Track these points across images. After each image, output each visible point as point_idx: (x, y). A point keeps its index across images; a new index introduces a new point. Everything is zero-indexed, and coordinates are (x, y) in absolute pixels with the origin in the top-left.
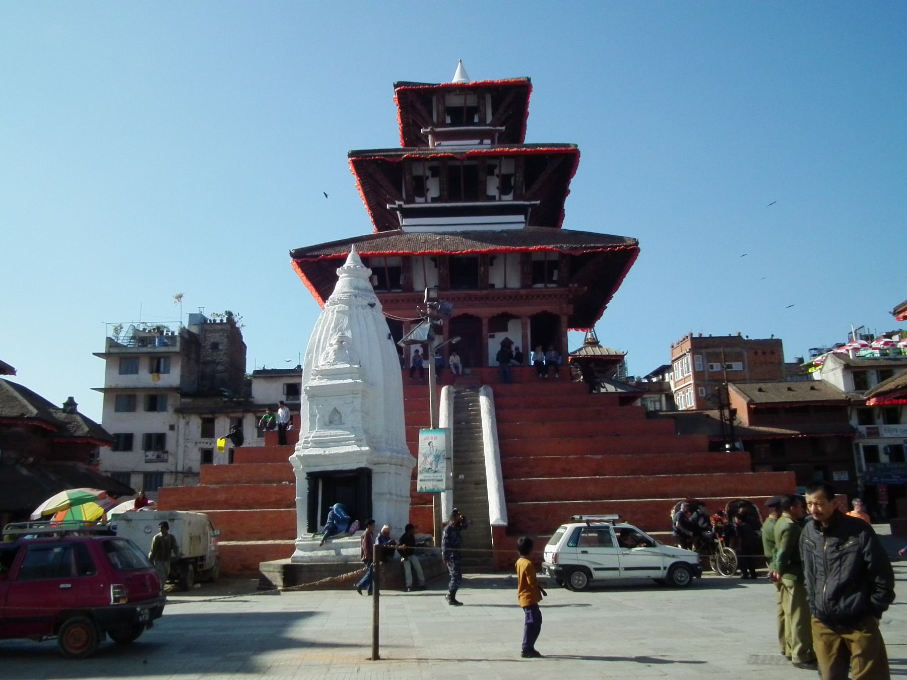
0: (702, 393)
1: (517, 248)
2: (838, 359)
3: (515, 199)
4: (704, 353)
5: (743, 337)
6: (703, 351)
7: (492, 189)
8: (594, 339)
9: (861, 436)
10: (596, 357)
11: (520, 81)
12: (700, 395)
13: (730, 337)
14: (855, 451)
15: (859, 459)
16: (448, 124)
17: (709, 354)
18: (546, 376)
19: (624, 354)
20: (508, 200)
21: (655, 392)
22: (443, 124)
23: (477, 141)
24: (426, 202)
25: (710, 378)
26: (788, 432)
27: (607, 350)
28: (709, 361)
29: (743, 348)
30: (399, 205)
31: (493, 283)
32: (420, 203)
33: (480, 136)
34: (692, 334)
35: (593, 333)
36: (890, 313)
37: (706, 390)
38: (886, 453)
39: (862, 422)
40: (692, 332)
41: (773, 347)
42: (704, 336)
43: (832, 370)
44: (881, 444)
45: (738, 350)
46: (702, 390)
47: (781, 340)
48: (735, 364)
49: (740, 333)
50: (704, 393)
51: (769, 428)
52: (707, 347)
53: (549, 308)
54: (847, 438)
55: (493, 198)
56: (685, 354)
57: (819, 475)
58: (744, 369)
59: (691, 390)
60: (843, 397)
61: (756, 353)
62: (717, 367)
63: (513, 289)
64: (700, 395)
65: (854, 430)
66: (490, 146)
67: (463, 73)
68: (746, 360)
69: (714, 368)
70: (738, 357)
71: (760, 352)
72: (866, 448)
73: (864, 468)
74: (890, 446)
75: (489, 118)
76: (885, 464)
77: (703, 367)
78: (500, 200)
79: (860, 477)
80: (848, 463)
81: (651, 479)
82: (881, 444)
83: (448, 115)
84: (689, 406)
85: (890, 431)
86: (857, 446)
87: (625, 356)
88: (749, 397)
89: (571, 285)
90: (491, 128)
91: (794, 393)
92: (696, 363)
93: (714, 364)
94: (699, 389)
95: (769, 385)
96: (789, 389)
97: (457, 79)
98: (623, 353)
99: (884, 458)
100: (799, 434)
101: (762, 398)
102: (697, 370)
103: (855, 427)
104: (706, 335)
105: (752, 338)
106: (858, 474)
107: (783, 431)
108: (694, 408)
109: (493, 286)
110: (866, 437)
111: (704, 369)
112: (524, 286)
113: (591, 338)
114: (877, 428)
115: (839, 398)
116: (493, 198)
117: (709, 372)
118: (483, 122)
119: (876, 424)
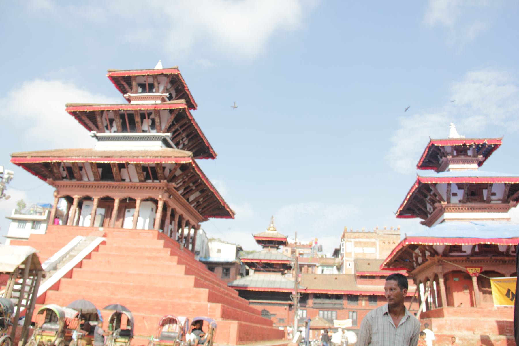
3: (158, 132)
6: (353, 240)
17: (356, 243)
20: (154, 133)
22: (136, 92)
24: (111, 132)
29: (376, 239)
30: (94, 134)
31: (124, 178)
32: (107, 134)
45: (373, 240)
58: (376, 252)
61: (384, 242)
71: (386, 243)
78: (149, 132)
83: (141, 87)
109: (124, 180)
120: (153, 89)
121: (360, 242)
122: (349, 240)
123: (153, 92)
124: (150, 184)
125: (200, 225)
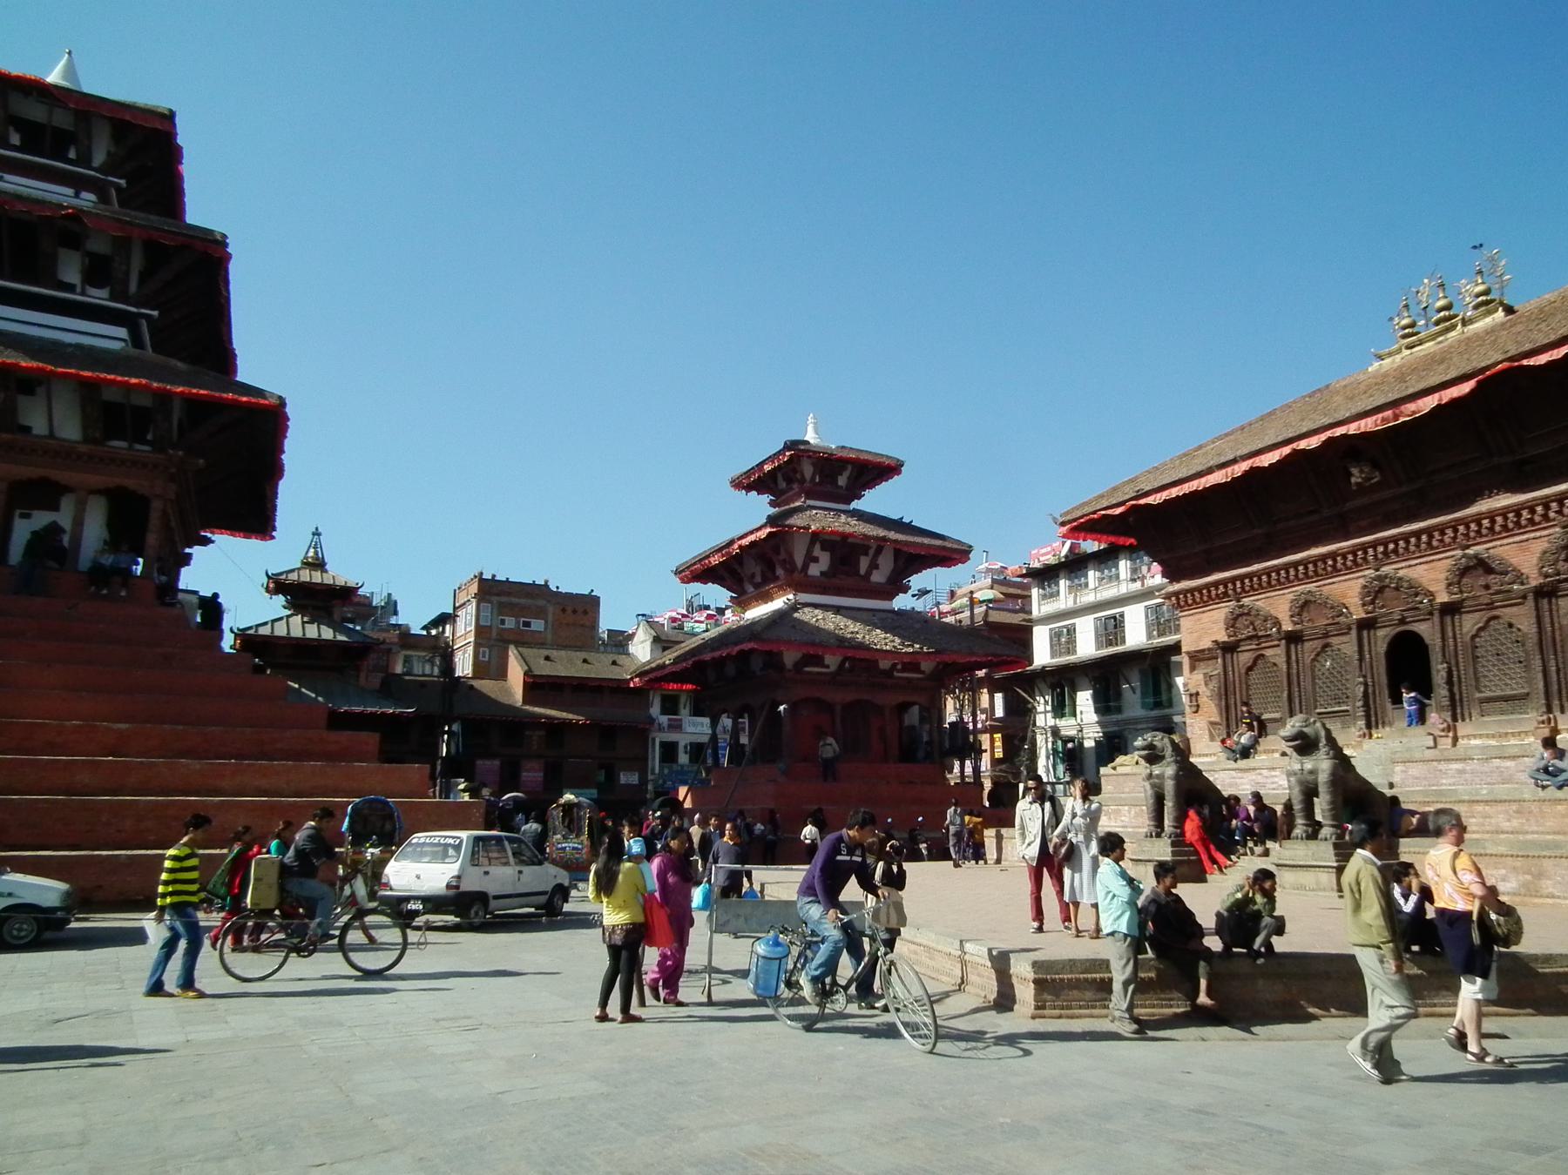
0: (484, 657)
1: (155, 385)
2: (649, 629)
3: (112, 298)
5: (550, 587)
6: (495, 599)
7: (71, 271)
8: (317, 559)
9: (661, 729)
10: (312, 585)
11: (146, 107)
12: (481, 658)
13: (534, 585)
14: (650, 750)
15: (654, 758)
16: (15, 145)
18: (105, 592)
19: (359, 585)
20: (98, 296)
23: (70, 191)
25: (498, 637)
26: (570, 716)
27: (333, 577)
29: (549, 601)
31: (27, 423)
33: (78, 184)
34: (481, 574)
35: (319, 550)
36: (672, 571)
37: (490, 652)
38: (686, 753)
39: (664, 711)
41: (588, 605)
43: (642, 642)
44: (683, 740)
45: (541, 602)
46: (484, 653)
47: (599, 598)
49: (546, 582)
50: (487, 656)
52: (498, 595)
53: (130, 484)
54: (641, 732)
55: (70, 288)
56: (469, 601)
57: (601, 777)
58: (546, 629)
59: (470, 649)
61: (564, 610)
62: (510, 623)
63: (64, 440)
64: (481, 658)
65: (652, 720)
66: (92, 204)
67: (70, 71)
68: (550, 618)
69: (506, 623)
70: (540, 613)
71: (569, 610)
72: (664, 745)
73: (657, 771)
74: (691, 744)
75: (99, 158)
76: (682, 766)
77: (491, 620)
78: (83, 293)
79: (652, 780)
80: (641, 764)
81: (196, 765)
82: (683, 740)
84: (466, 672)
85: (694, 725)
86: (654, 740)
87: (360, 590)
88: (528, 666)
89: (171, 452)
90: (98, 175)
93: (506, 618)
94: (481, 650)
95: (563, 653)
96: (585, 661)
97: (54, 77)
98: (357, 584)
99: (683, 758)
101: (544, 669)
103: (654, 716)
105: (562, 590)
106: (650, 777)
107: (564, 715)
108: (470, 676)
112: (86, 440)
113: (312, 557)
114: (681, 720)
116: (70, 288)
117: (498, 628)
118: (85, 160)
120: (67, 150)
121: (512, 606)
122: (488, 597)
123: (70, 162)
124: (144, 454)
125: (189, 556)
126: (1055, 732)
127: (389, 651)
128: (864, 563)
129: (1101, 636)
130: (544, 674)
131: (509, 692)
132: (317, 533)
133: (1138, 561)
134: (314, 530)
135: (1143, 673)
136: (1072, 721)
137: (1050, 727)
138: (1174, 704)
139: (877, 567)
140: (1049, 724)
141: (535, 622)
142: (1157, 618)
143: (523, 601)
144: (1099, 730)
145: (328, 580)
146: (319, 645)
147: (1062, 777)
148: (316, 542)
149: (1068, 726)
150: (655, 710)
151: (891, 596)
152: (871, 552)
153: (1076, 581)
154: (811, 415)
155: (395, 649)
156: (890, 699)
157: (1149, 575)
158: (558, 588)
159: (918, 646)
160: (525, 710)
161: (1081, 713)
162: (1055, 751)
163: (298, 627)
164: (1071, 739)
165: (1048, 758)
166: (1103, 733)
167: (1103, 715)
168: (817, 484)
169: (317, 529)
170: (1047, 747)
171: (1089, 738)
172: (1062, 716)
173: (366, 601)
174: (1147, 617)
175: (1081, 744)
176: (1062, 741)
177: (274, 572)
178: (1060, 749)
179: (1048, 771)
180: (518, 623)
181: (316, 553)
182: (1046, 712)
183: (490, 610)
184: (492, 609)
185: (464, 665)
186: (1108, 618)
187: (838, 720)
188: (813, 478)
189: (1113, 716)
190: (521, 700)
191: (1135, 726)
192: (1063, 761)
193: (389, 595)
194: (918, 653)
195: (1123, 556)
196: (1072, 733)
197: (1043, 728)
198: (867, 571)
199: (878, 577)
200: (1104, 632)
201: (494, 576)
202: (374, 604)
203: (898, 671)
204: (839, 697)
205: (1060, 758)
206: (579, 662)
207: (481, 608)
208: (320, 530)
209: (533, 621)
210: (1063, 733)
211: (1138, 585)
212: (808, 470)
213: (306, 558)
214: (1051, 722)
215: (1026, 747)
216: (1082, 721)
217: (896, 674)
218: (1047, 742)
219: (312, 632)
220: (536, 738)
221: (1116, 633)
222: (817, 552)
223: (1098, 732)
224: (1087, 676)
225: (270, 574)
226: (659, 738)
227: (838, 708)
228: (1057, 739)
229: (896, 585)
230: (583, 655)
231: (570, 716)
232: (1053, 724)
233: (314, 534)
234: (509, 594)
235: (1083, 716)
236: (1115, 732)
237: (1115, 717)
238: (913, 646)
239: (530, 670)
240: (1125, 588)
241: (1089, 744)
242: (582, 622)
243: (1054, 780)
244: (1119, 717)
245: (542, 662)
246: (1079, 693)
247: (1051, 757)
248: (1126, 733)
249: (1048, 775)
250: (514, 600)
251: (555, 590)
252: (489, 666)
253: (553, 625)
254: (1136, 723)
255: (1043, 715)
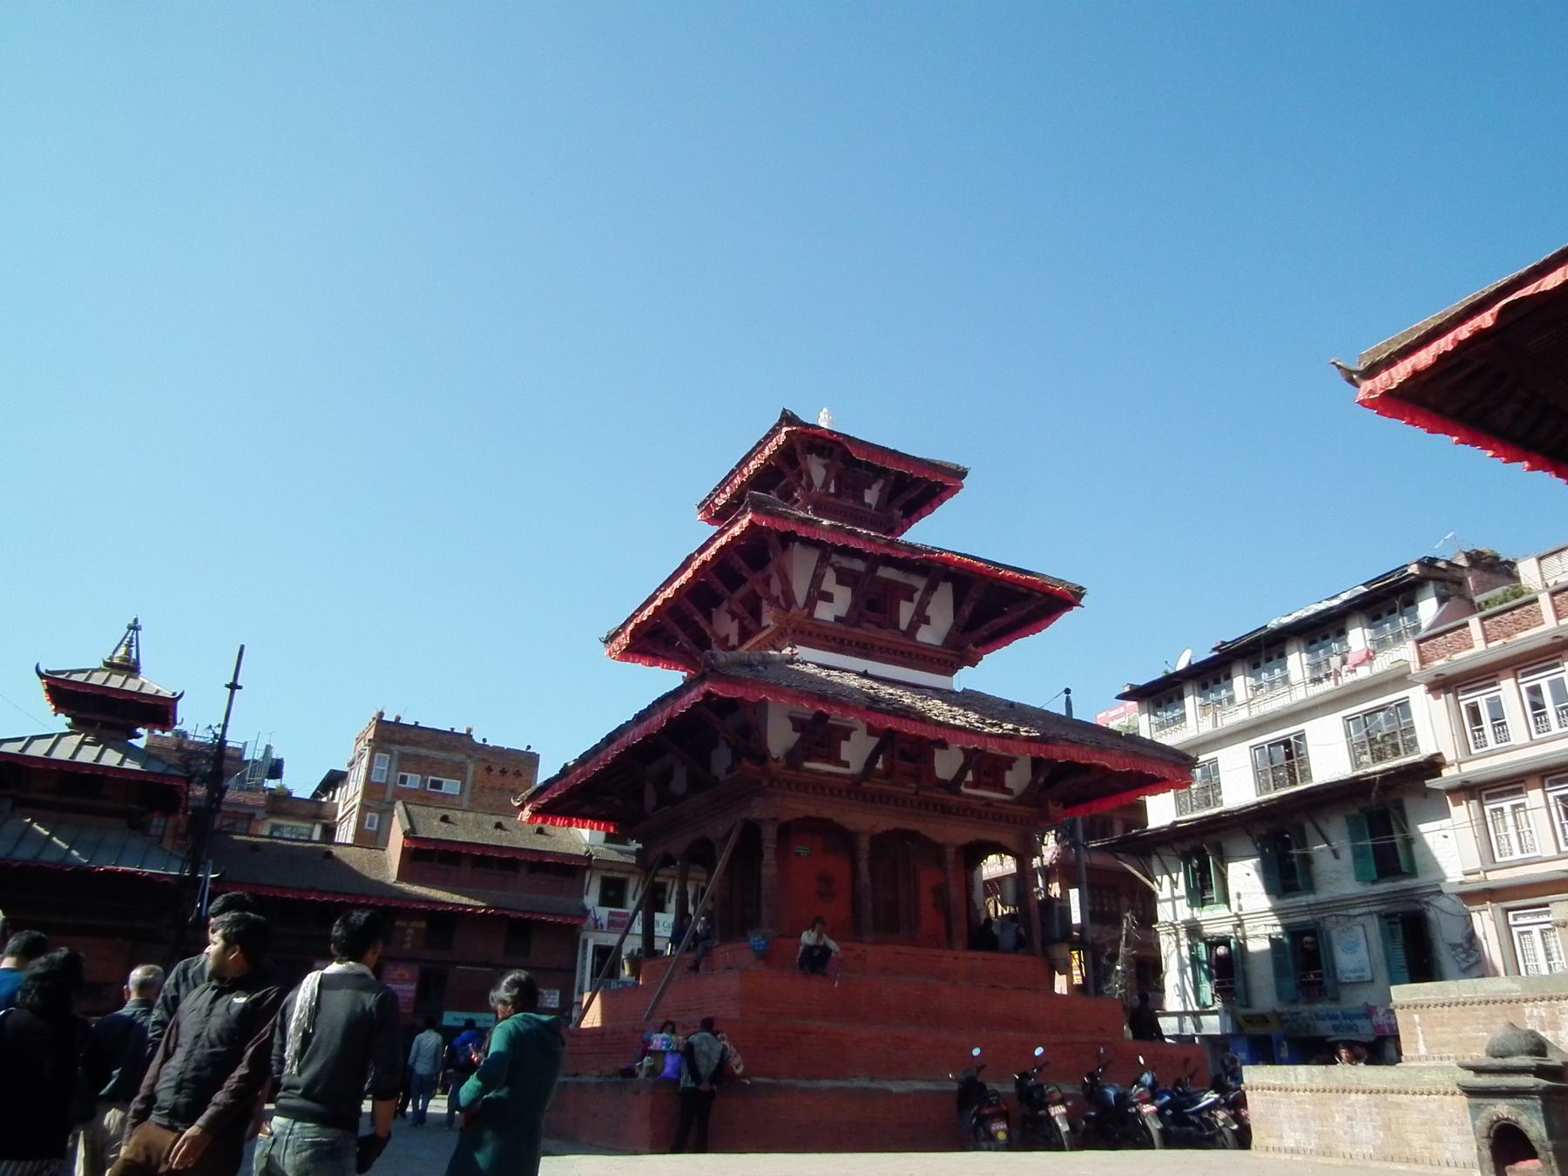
4: (395, 752)
6: (396, 749)
9: (597, 927)
12: (366, 827)
13: (452, 733)
14: (579, 959)
21: (304, 818)
26: (465, 900)
28: (400, 769)
29: (469, 756)
34: (381, 714)
35: (134, 649)
37: (380, 819)
39: (604, 901)
40: (384, 712)
42: (403, 721)
45: (459, 757)
46: (372, 819)
47: (538, 755)
48: (447, 782)
49: (469, 730)
51: (422, 888)
52: (401, 743)
58: (462, 792)
60: (582, 851)
61: (489, 769)
62: (414, 781)
65: (584, 913)
69: (408, 782)
70: (457, 771)
71: (496, 770)
77: (388, 776)
86: (586, 941)
91: (503, 833)
92: (375, 767)
94: (368, 815)
100: (482, 907)
101: (434, 829)
102: (374, 779)
103: (589, 907)
104: (407, 720)
107: (457, 898)
110: (605, 929)
111: (387, 781)
115: (573, 851)
119: (625, 908)
121: (419, 759)
122: (386, 745)
126: (1193, 930)
127: (251, 817)
128: (906, 612)
129: (1264, 772)
130: (433, 837)
131: (383, 865)
132: (134, 627)
133: (1321, 652)
134: (131, 622)
135: (1352, 823)
136: (1222, 911)
137: (1183, 922)
138: (1419, 871)
139: (927, 621)
140: (1181, 918)
141: (447, 783)
142: (1368, 733)
143: (434, 753)
144: (1277, 922)
145: (132, 685)
146: (95, 776)
147: (1209, 1002)
148: (131, 638)
149: (1215, 920)
150: (591, 899)
151: (950, 669)
152: (917, 596)
153: (1212, 696)
154: (825, 410)
155: (260, 814)
156: (957, 834)
157: (1345, 668)
158: (484, 740)
159: (1010, 726)
160: (401, 892)
161: (1239, 896)
162: (1195, 960)
163: (77, 749)
164: (1224, 941)
165: (1182, 971)
166: (1282, 925)
167: (1279, 897)
168: (831, 495)
169: (136, 621)
170: (1179, 953)
171: (1256, 936)
172: (1203, 903)
173: (237, 754)
174: (1348, 734)
175: (1242, 948)
176: (1207, 944)
177: (50, 669)
178: (1204, 957)
179: (1183, 993)
180: (424, 781)
181: (128, 653)
182: (1174, 899)
183: (387, 762)
184: (390, 761)
185: (346, 833)
186: (1274, 744)
187: (863, 865)
188: (826, 485)
189: (1298, 899)
190: (396, 876)
191: (1345, 913)
192: (1210, 978)
193: (268, 748)
194: (1011, 737)
195: (1295, 644)
196: (1226, 929)
197: (1172, 924)
198: (910, 624)
199: (929, 636)
200: (1268, 767)
201: (398, 718)
202: (246, 757)
203: (968, 785)
204: (866, 821)
205: (1204, 970)
206: (490, 828)
207: (376, 759)
208: (139, 623)
209: (445, 780)
210: (1208, 930)
211: (1328, 685)
212: (817, 470)
213: (111, 658)
214: (1184, 912)
215: (1119, 968)
216: (1240, 908)
217: (964, 790)
218: (1178, 946)
219: (88, 755)
220: (411, 931)
221: (1291, 766)
222: (829, 583)
223: (1275, 925)
224: (1249, 834)
225: (43, 671)
226: (593, 940)
227: (864, 843)
228: (1197, 940)
229: (960, 651)
230: (495, 819)
231: (465, 900)
232: (1188, 917)
233: (130, 628)
234: (416, 743)
235: (1242, 901)
236: (1303, 924)
237: (1304, 900)
238: (1001, 727)
239: (413, 829)
240: (1301, 693)
241: (1258, 945)
242: (512, 787)
243: (1196, 1009)
244: (1311, 898)
245: (436, 823)
246: (1231, 866)
247: (1189, 970)
248: (1328, 924)
249: (1184, 1001)
250: (423, 752)
251: (482, 742)
252: (370, 838)
253: (472, 788)
254: (1347, 907)
255: (1170, 903)
